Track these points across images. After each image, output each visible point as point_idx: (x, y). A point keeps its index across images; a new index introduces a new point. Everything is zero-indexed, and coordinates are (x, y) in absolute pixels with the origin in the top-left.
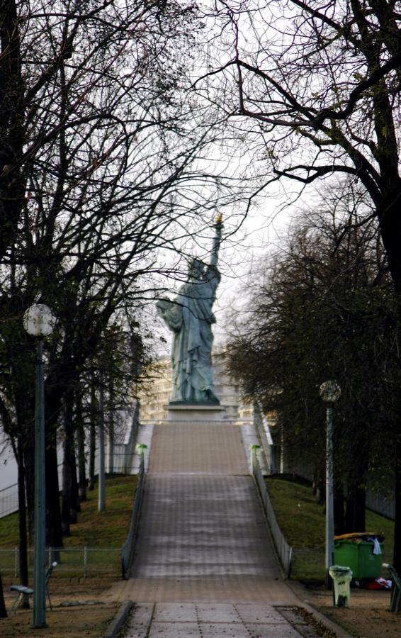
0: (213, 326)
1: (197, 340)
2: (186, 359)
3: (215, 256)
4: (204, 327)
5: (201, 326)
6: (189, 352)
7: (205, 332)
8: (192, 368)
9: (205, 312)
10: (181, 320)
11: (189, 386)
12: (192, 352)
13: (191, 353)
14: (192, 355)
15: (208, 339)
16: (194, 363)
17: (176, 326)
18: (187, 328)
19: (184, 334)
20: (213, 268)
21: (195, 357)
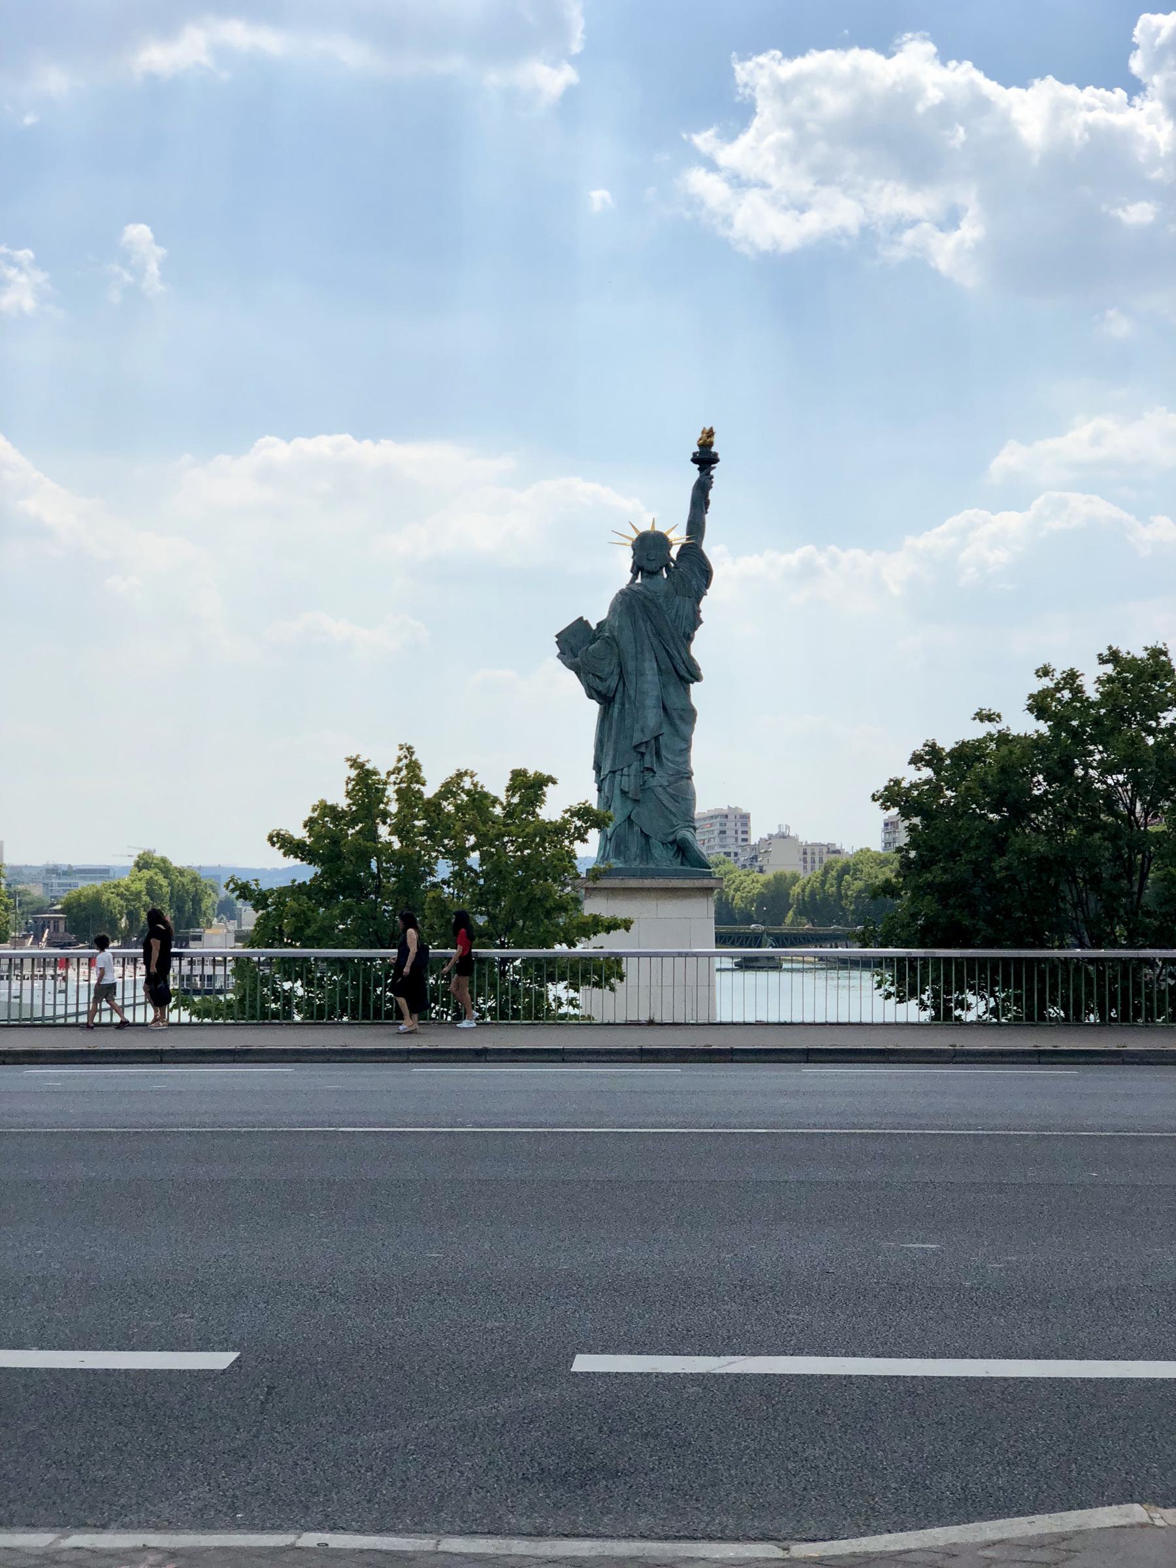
0: (694, 688)
1: (652, 717)
2: (629, 766)
3: (696, 527)
4: (671, 689)
5: (664, 686)
6: (636, 747)
7: (674, 701)
8: (644, 788)
9: (674, 652)
10: (617, 671)
11: (636, 828)
12: (643, 750)
13: (638, 750)
14: (643, 754)
15: (681, 718)
16: (648, 775)
17: (601, 687)
18: (632, 693)
19: (623, 704)
20: (693, 554)
21: (649, 760)
